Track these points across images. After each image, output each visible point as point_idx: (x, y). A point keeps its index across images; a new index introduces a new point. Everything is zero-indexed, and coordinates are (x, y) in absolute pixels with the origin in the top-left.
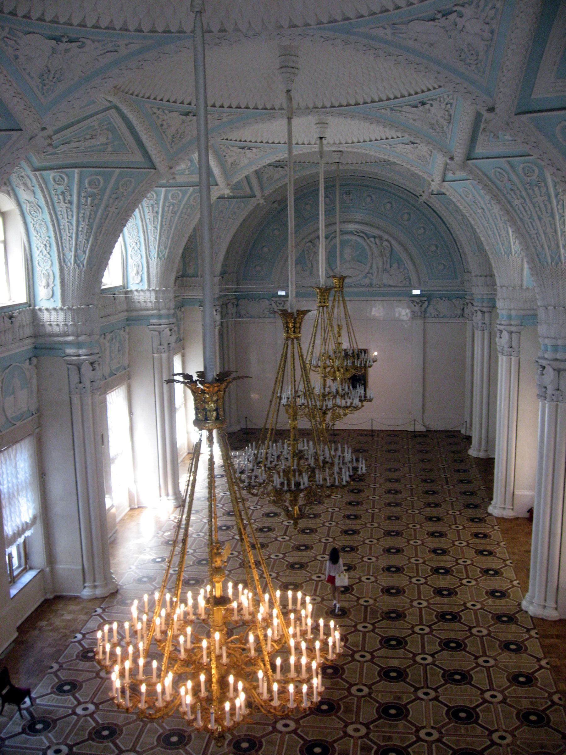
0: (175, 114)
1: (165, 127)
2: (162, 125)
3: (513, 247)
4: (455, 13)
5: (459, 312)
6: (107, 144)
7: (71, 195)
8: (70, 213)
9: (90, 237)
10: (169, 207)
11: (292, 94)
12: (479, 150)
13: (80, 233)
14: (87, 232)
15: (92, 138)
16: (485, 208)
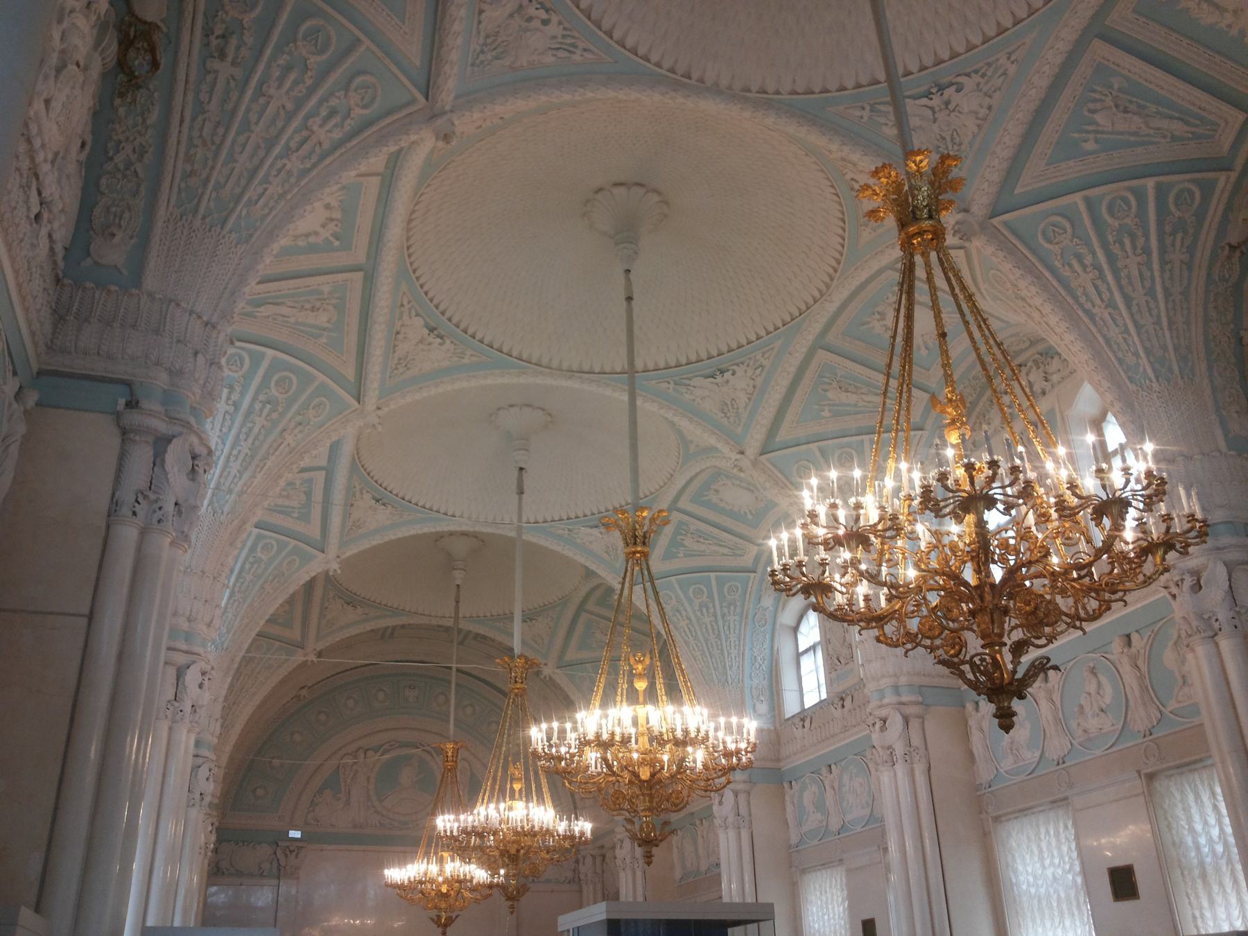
0: (419, 322)
1: (400, 337)
2: (398, 333)
3: (729, 672)
4: (953, 88)
5: (570, 875)
6: (324, 329)
7: (242, 394)
8: (228, 423)
9: (246, 469)
10: (252, 564)
11: (632, 276)
12: (783, 435)
13: (232, 459)
14: (244, 460)
15: (313, 309)
16: (693, 619)
